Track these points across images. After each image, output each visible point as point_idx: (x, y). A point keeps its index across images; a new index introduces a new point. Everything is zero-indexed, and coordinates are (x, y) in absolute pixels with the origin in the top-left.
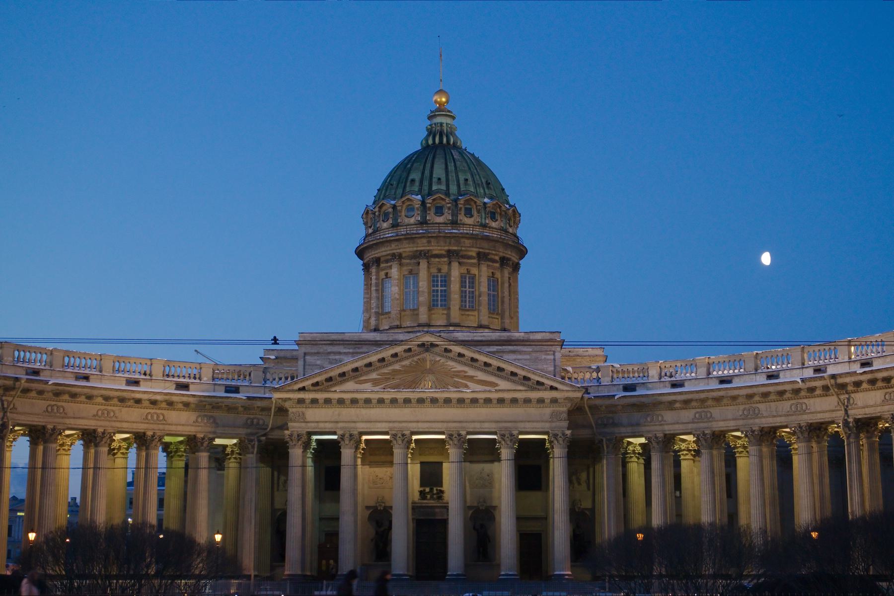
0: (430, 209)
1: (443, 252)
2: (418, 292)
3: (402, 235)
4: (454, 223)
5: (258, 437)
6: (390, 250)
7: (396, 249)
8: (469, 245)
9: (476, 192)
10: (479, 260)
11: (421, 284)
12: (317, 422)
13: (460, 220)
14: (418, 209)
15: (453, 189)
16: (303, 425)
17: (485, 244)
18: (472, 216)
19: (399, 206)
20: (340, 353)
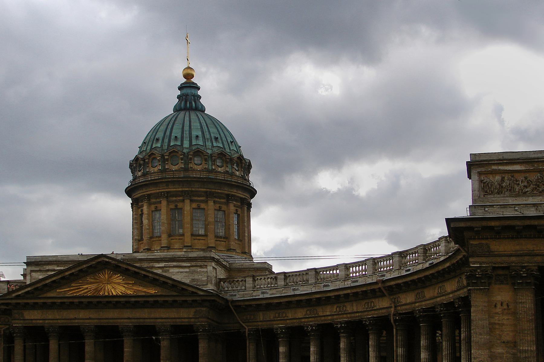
0: (167, 160)
4: (186, 170)
5: (4, 331)
6: (142, 193)
9: (204, 146)
10: (207, 198)
12: (32, 320)
13: (191, 167)
14: (159, 161)
15: (186, 144)
16: (22, 322)
19: (147, 159)
20: (54, 270)
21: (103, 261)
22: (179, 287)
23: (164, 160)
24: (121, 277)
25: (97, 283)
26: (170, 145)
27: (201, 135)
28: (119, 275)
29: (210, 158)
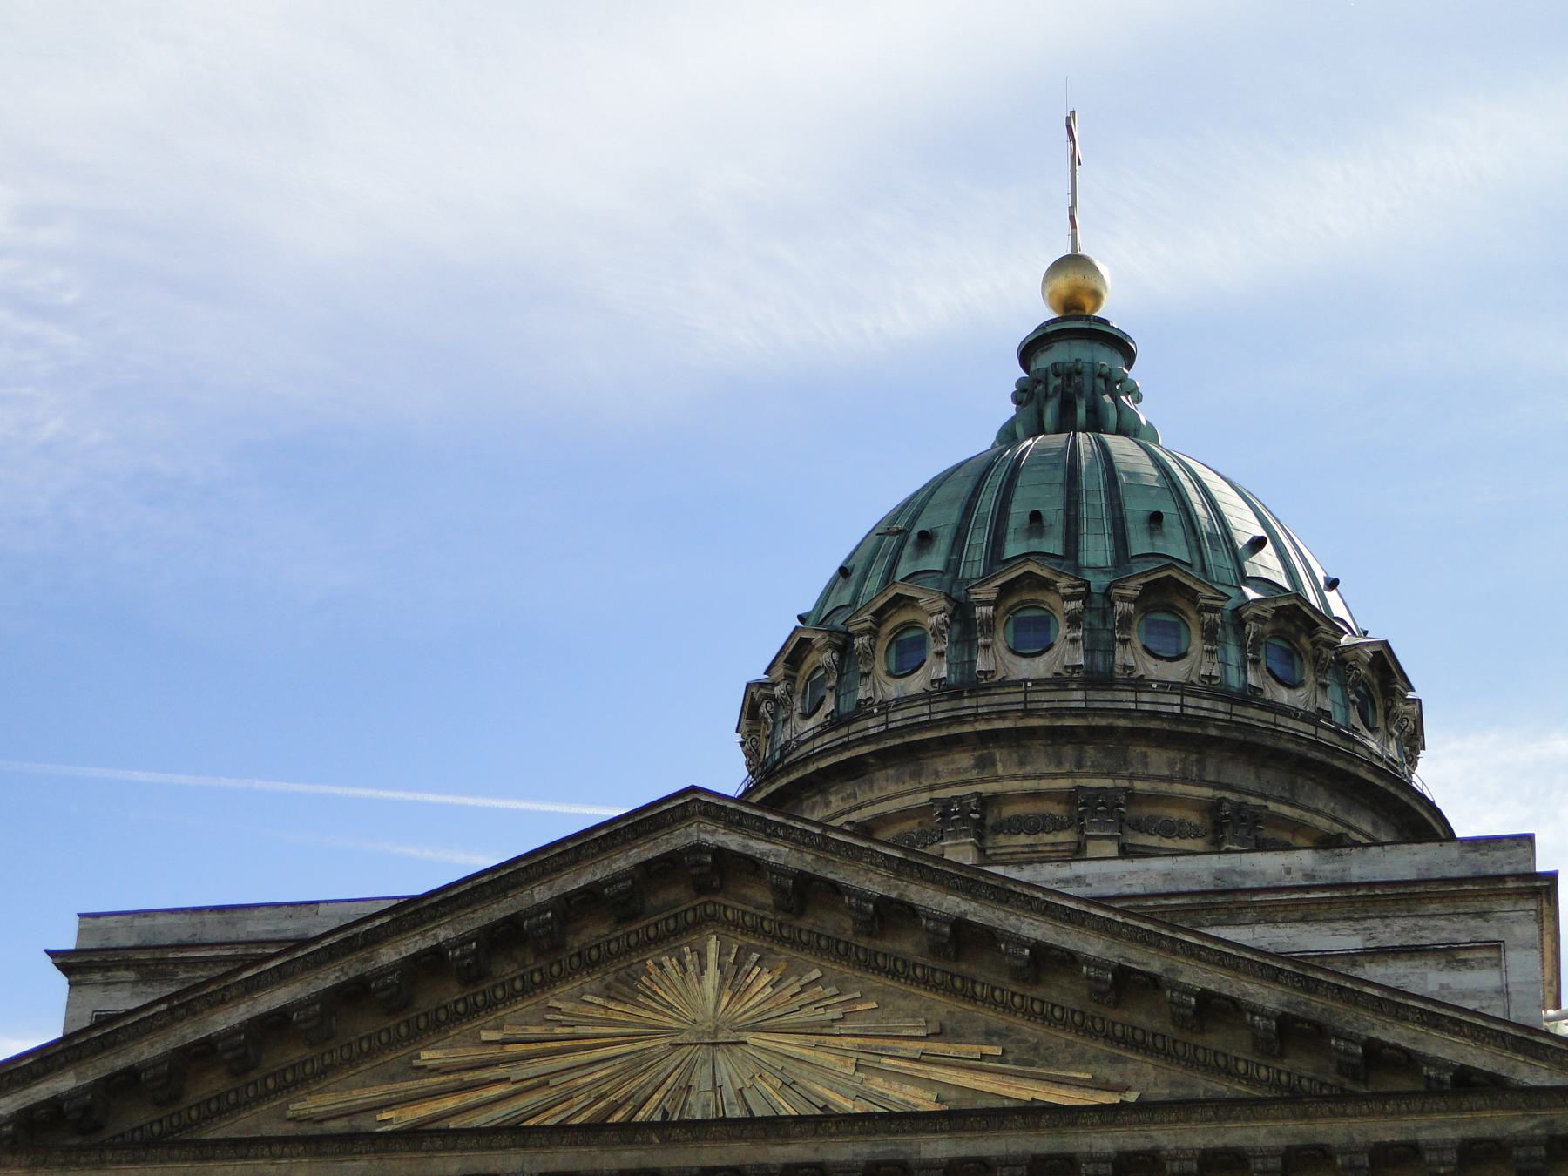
0: (989, 626)
1: (1057, 810)
3: (865, 740)
4: (1097, 678)
7: (848, 812)
8: (1167, 772)
9: (1198, 566)
13: (1125, 667)
14: (938, 634)
15: (1096, 550)
17: (1241, 774)
18: (1182, 656)
19: (860, 634)
21: (698, 848)
22: (1338, 1037)
24: (833, 990)
26: (1001, 553)
27: (1176, 518)
28: (816, 974)
29: (1230, 630)
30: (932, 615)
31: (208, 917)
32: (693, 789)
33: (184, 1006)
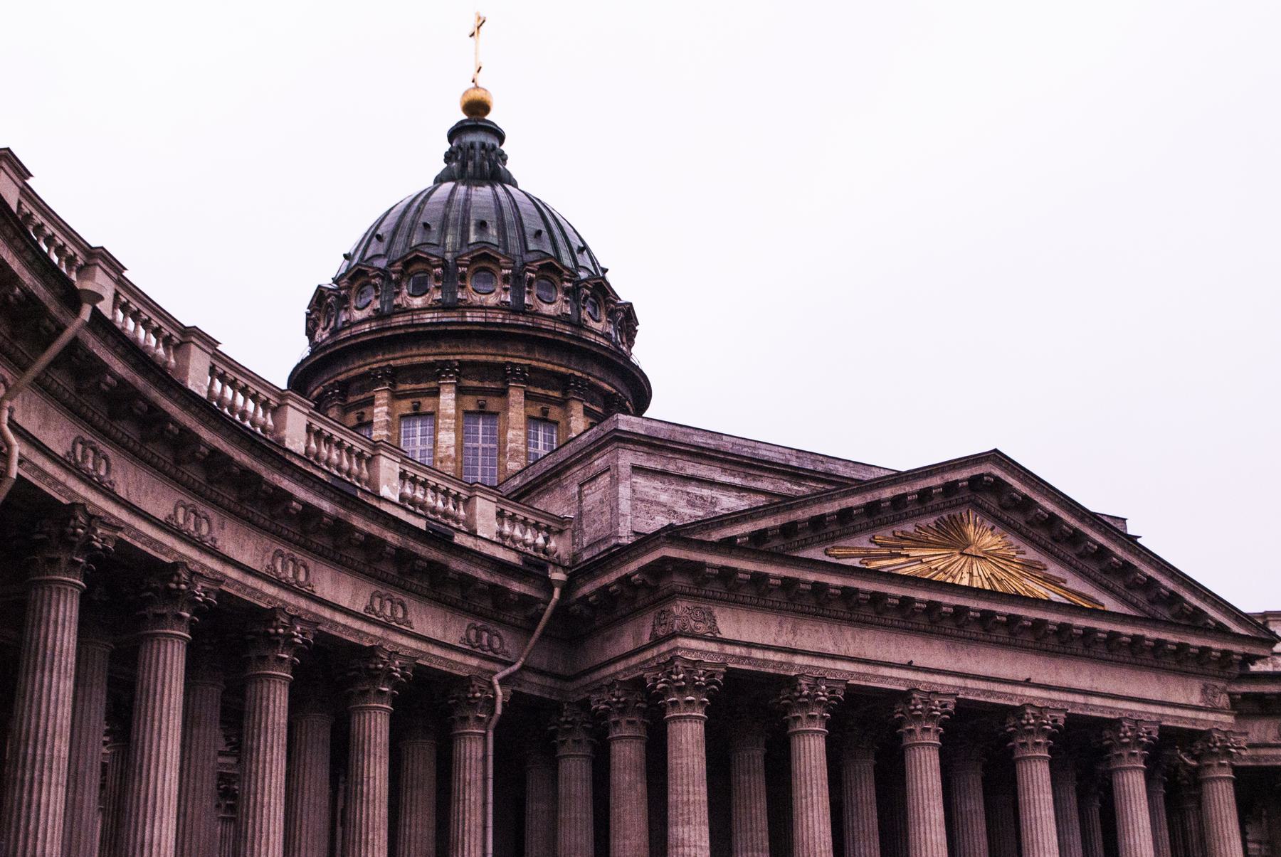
2: (501, 451)
3: (477, 324)
6: (435, 355)
8: (598, 375)
11: (510, 434)
12: (749, 645)
13: (585, 320)
14: (506, 279)
15: (567, 262)
16: (713, 647)
18: (599, 321)
19: (462, 266)
20: (712, 483)
21: (990, 475)
23: (517, 282)
25: (946, 547)
26: (526, 246)
30: (505, 269)
31: (678, 428)
32: (995, 450)
33: (818, 498)
